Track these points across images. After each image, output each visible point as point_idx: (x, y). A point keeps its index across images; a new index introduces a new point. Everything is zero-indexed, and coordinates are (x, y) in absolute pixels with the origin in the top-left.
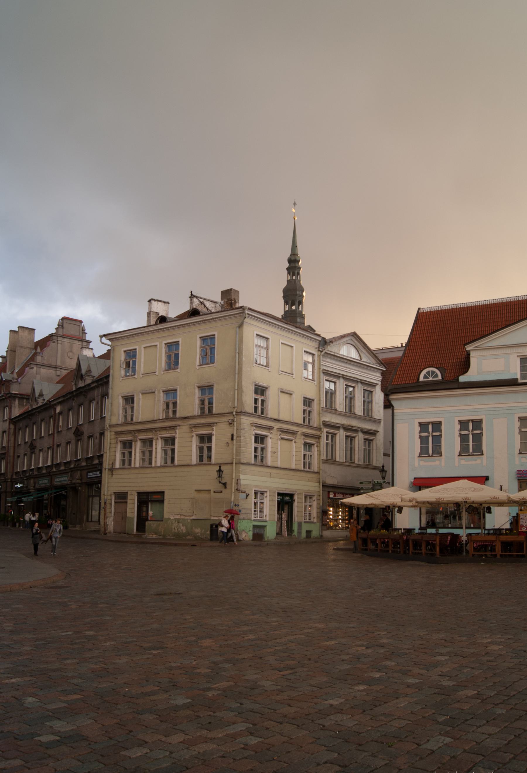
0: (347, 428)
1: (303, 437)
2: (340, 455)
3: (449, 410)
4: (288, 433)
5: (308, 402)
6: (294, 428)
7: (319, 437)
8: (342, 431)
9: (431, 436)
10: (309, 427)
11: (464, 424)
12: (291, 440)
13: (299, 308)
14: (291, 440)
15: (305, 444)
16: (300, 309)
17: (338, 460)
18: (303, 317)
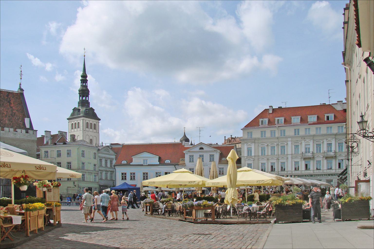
0: (106, 171)
1: (94, 174)
2: (104, 178)
3: (128, 170)
4: (90, 173)
5: (95, 165)
6: (92, 172)
7: (98, 174)
8: (104, 171)
9: (124, 177)
10: (96, 171)
11: (131, 174)
12: (91, 175)
13: (86, 99)
14: (91, 175)
15: (95, 175)
16: (87, 99)
17: (103, 179)
18: (89, 103)
